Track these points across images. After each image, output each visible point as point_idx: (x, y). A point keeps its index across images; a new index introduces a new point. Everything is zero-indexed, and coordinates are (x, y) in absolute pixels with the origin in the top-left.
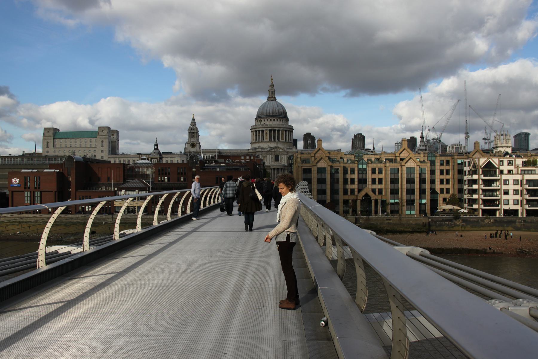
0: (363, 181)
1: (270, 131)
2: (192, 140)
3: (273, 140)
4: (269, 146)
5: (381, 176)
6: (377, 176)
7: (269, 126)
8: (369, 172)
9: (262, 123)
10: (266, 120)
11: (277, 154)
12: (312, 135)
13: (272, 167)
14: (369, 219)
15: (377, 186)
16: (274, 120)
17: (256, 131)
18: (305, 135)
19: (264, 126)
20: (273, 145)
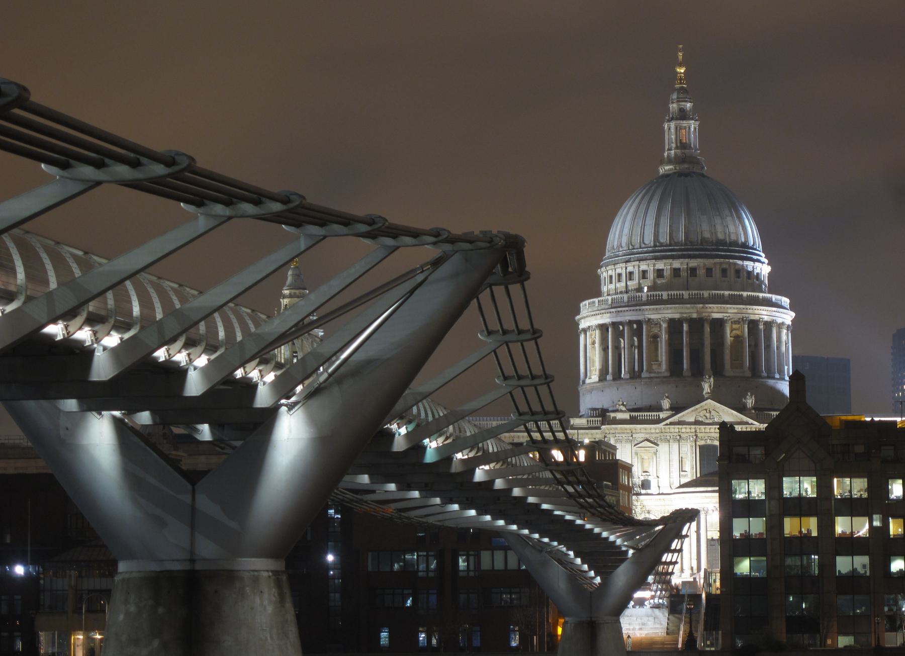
17: (603, 328)
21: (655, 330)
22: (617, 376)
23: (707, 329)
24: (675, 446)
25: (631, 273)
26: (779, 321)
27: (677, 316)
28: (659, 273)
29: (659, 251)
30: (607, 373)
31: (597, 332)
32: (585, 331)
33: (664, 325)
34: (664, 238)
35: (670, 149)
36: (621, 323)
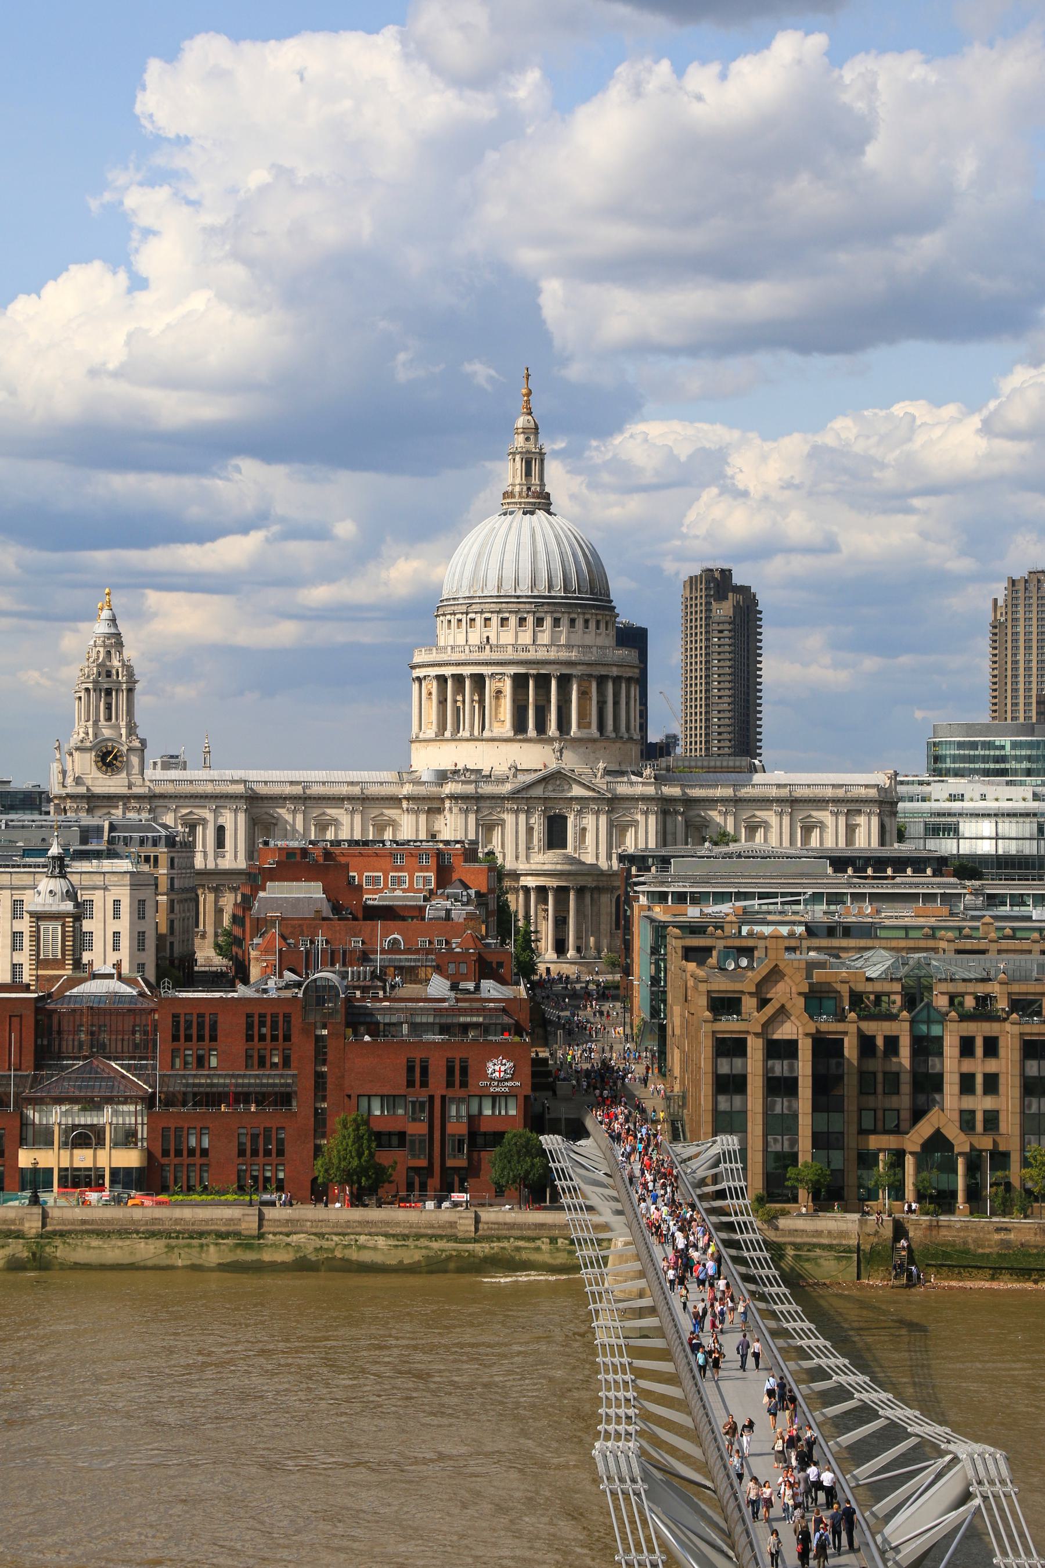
0: (928, 1085)
1: (520, 682)
2: (107, 733)
3: (531, 732)
5: (992, 1066)
6: (979, 1066)
7: (509, 654)
8: (951, 1048)
9: (475, 638)
10: (495, 620)
12: (737, 580)
13: (531, 882)
14: (939, 1226)
15: (981, 1103)
16: (539, 622)
17: (442, 679)
18: (692, 581)
19: (487, 655)
20: (534, 757)
23: (554, 683)
25: (473, 620)
30: (445, 729)
31: (435, 683)
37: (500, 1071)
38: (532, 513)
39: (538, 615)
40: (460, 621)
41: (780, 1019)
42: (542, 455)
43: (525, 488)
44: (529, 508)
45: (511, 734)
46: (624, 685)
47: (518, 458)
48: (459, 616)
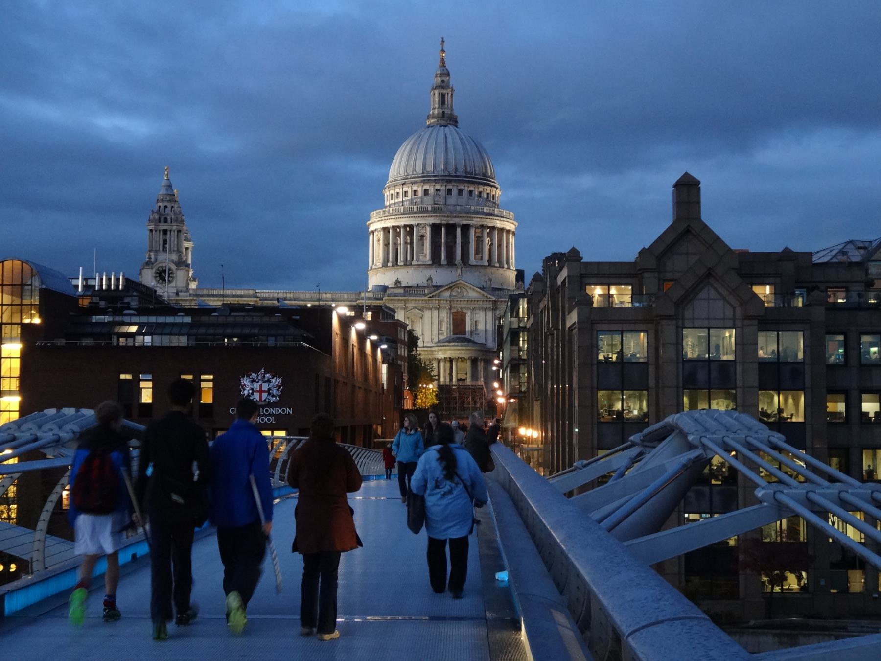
4: (430, 279)
11: (458, 306)
17: (386, 230)
21: (422, 232)
22: (395, 263)
23: (459, 231)
24: (436, 313)
25: (406, 192)
26: (508, 228)
27: (438, 222)
28: (426, 192)
29: (426, 178)
30: (388, 261)
31: (382, 232)
32: (373, 232)
33: (428, 229)
34: (430, 168)
35: (434, 109)
36: (399, 227)
37: (261, 391)
38: (445, 126)
39: (448, 187)
40: (398, 193)
41: (703, 294)
42: (452, 90)
43: (441, 111)
44: (443, 123)
45: (430, 263)
46: (505, 234)
47: (436, 92)
48: (397, 190)
